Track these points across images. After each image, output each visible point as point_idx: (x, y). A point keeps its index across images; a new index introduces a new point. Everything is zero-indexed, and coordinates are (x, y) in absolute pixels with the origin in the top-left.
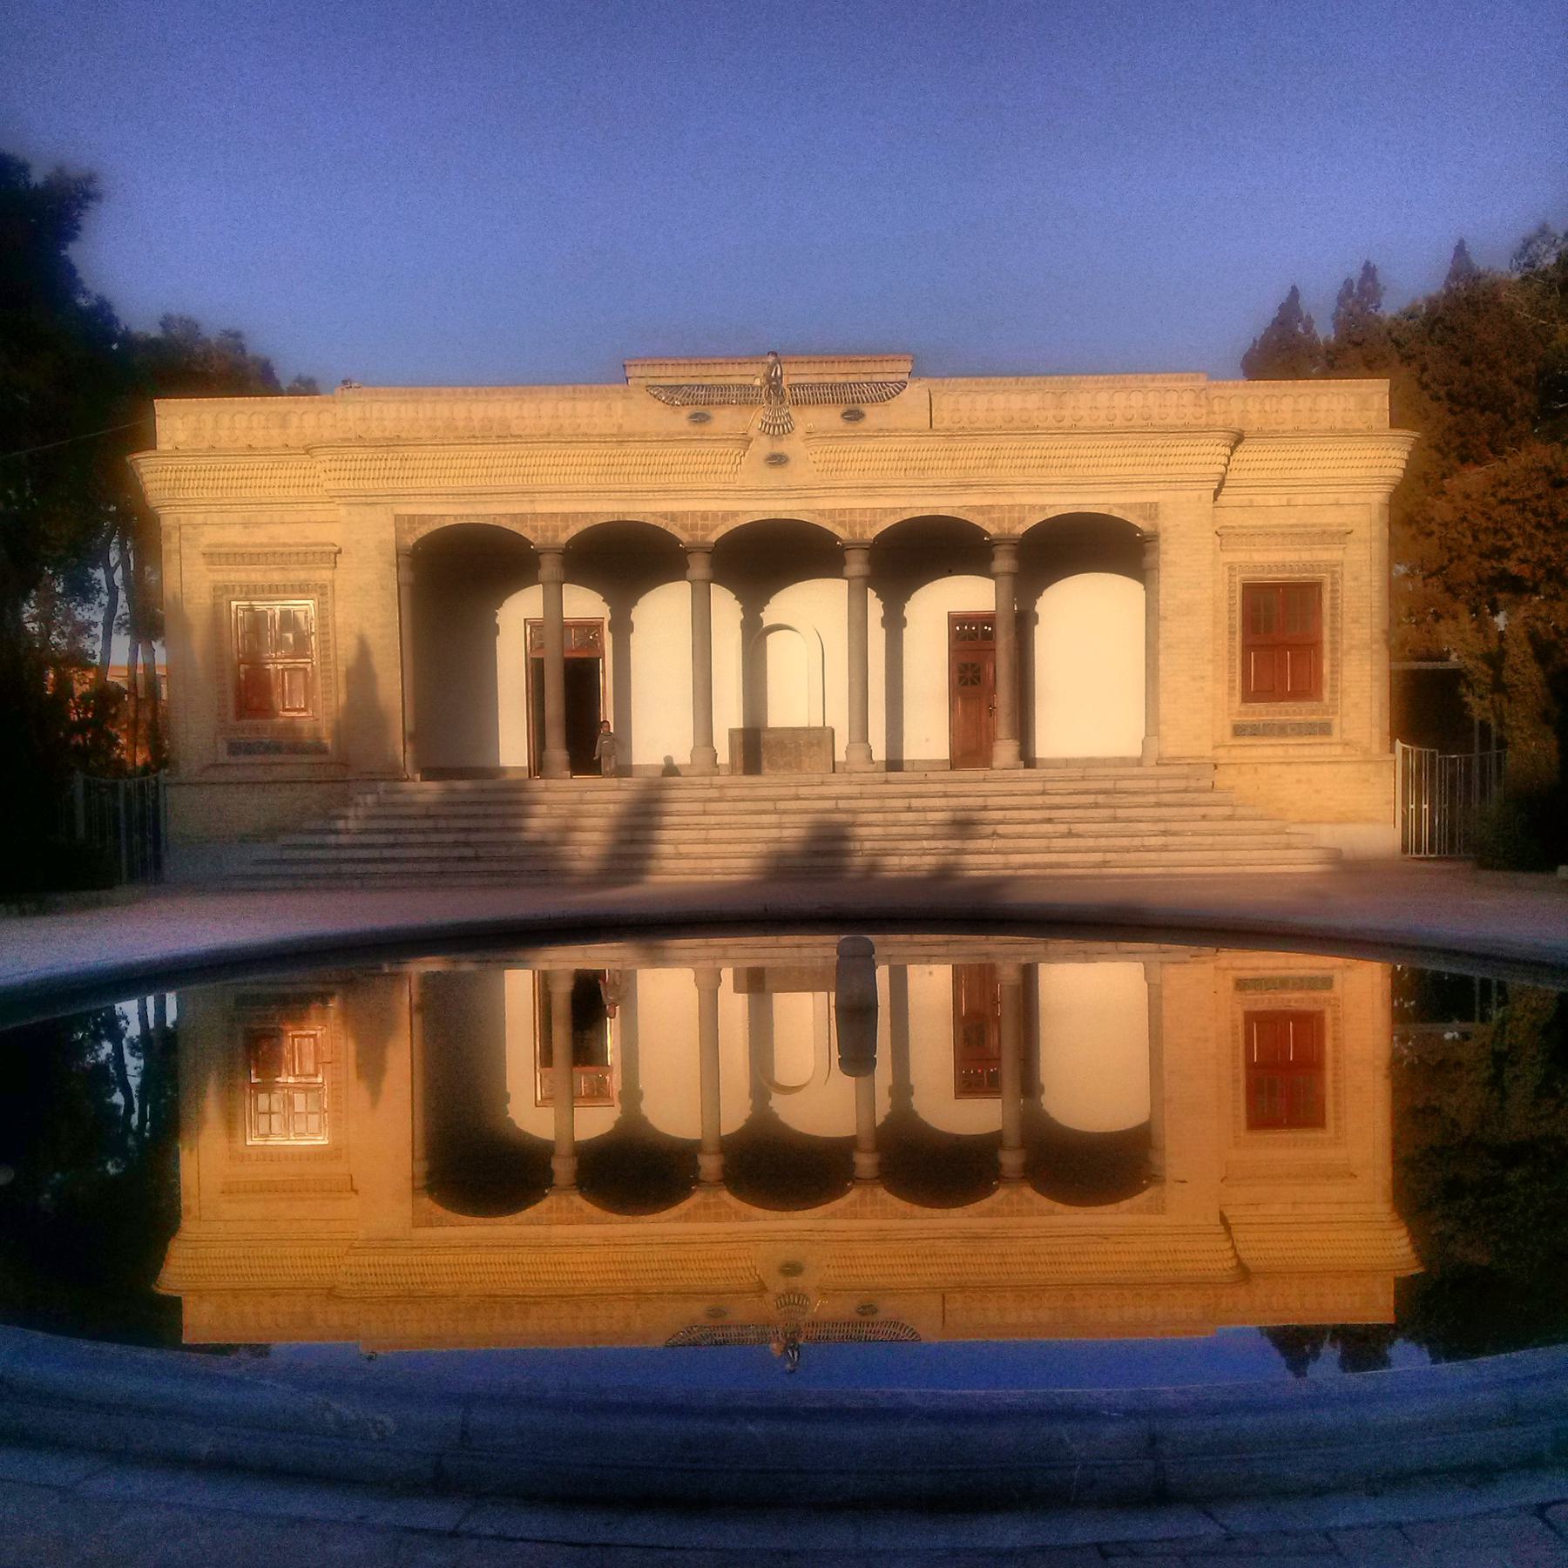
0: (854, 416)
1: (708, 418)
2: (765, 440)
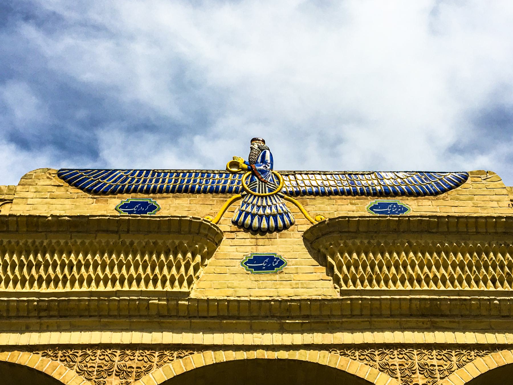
1: (153, 208)
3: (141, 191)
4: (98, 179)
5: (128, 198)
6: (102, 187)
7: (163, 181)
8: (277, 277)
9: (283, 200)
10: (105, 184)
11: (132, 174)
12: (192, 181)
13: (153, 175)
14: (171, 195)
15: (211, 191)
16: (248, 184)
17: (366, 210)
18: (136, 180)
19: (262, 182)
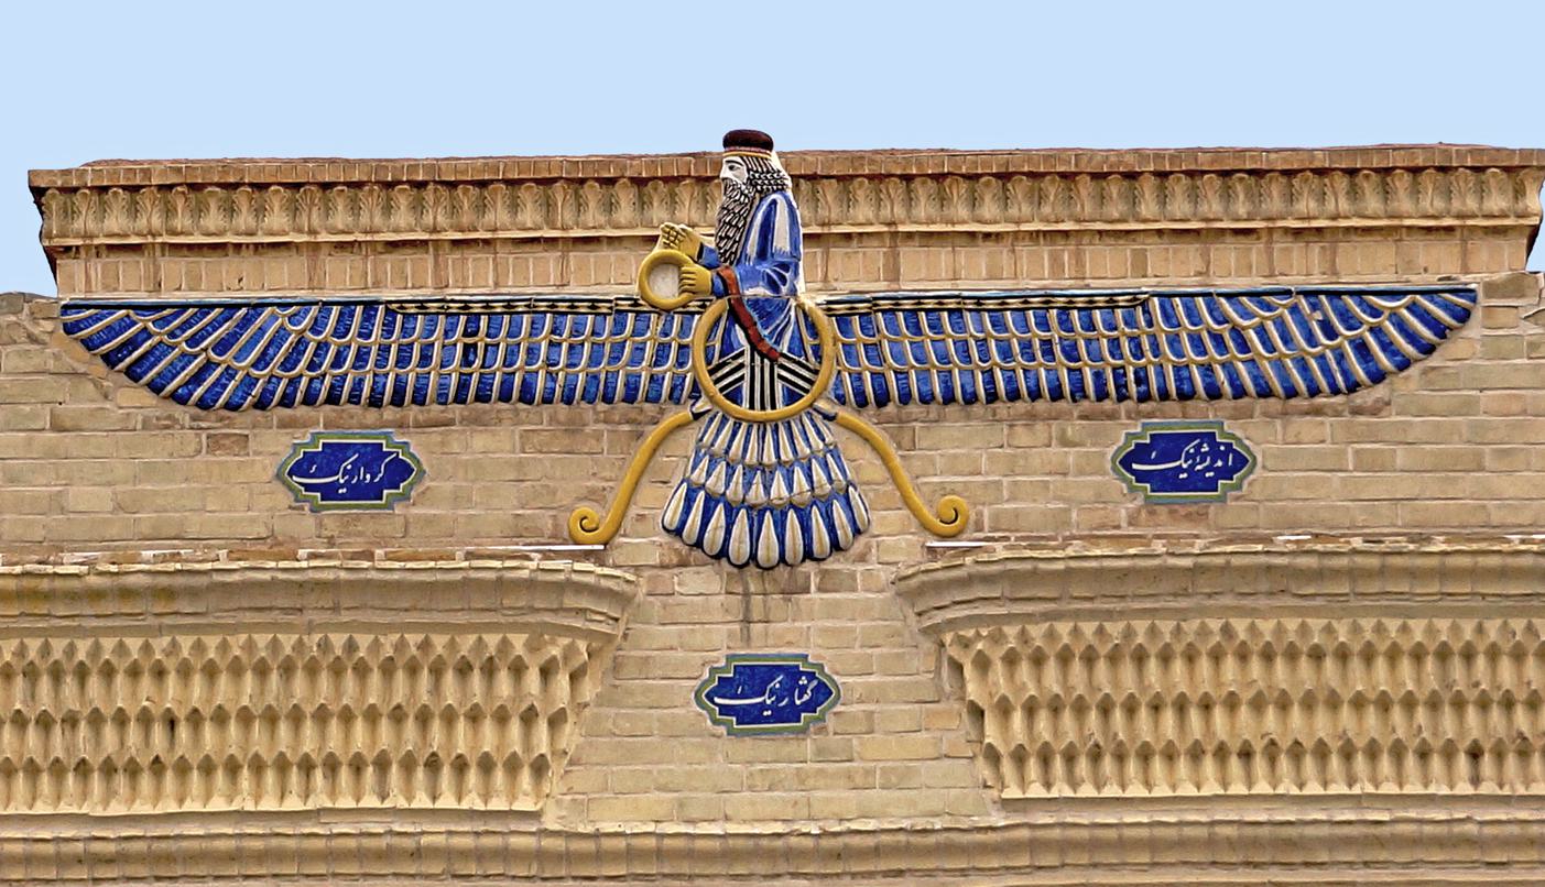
0: (1182, 467)
1: (400, 471)
2: (701, 583)
3: (354, 398)
4: (205, 350)
5: (315, 428)
6: (221, 384)
7: (425, 359)
8: (808, 746)
9: (831, 433)
10: (230, 373)
11: (316, 328)
13: (388, 329)
14: (456, 410)
15: (588, 397)
16: (715, 362)
17: (1109, 466)
18: (333, 349)
19: (763, 356)
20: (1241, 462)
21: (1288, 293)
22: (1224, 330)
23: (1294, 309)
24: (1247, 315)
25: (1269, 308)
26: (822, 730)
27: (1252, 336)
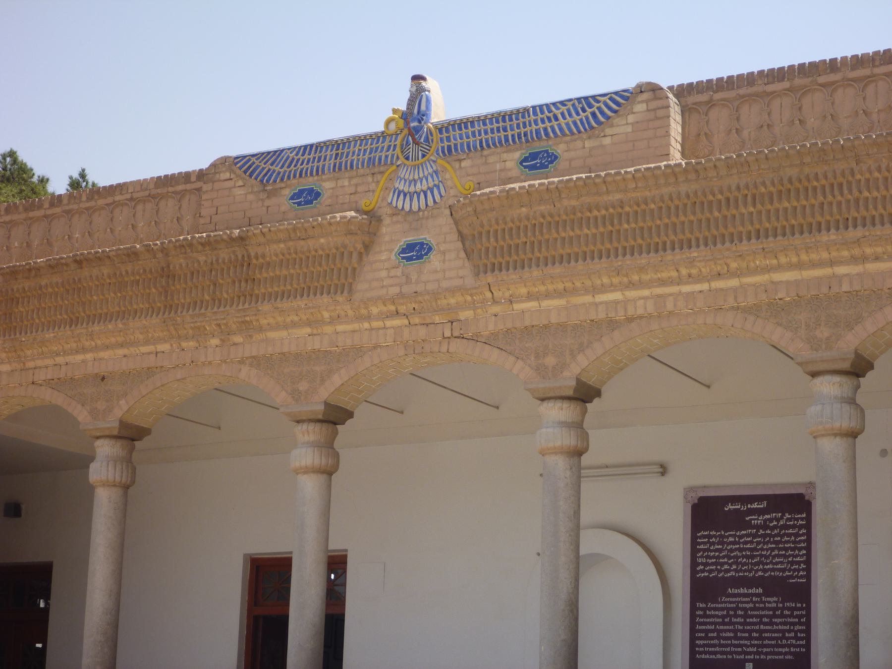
1: (318, 195)
10: (274, 171)
11: (297, 155)
12: (351, 154)
20: (556, 157)
21: (570, 100)
22: (551, 115)
23: (573, 105)
24: (558, 109)
25: (565, 105)
26: (429, 262)
27: (560, 116)
